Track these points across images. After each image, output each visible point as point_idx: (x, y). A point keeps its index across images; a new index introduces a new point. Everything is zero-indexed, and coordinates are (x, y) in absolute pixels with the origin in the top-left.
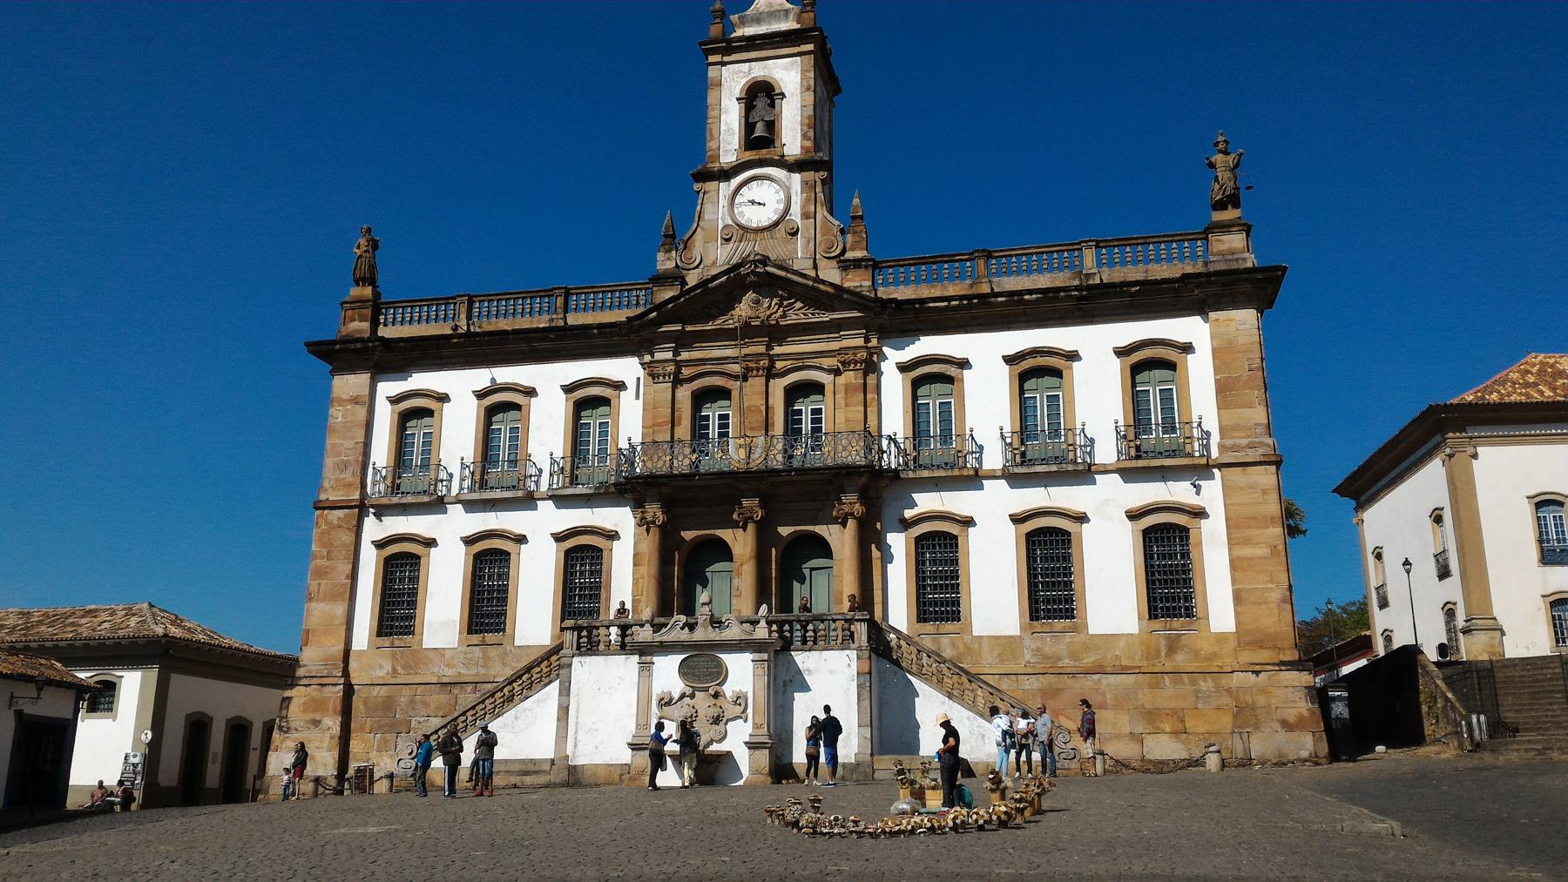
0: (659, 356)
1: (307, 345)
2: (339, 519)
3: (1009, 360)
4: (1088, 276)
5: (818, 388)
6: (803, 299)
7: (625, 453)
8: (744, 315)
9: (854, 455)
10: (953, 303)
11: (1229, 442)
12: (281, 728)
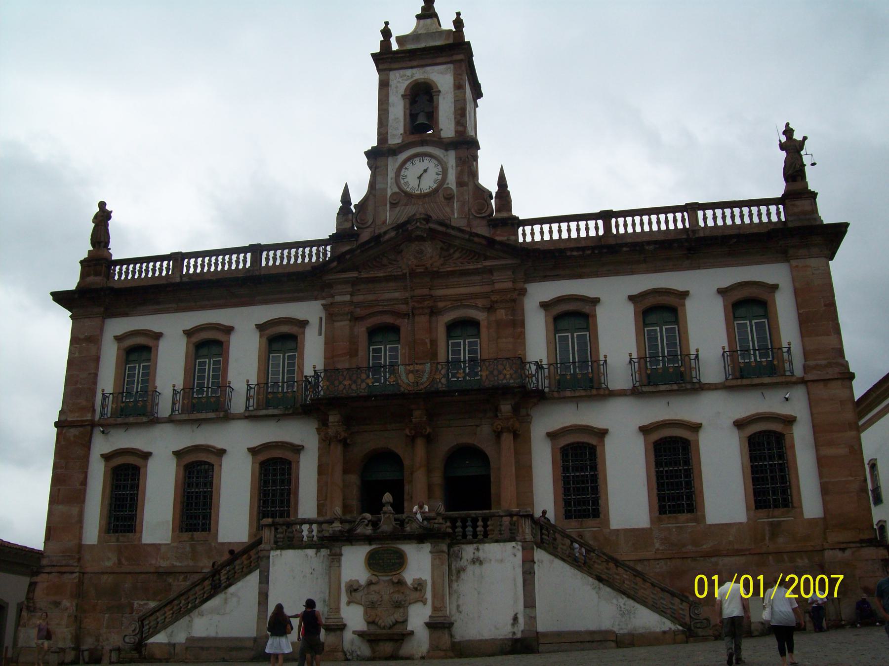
0: (338, 298)
1: (53, 294)
2: (75, 436)
3: (631, 298)
4: (694, 231)
5: (474, 324)
6: (460, 250)
7: (310, 380)
8: (410, 263)
9: (508, 377)
10: (589, 252)
11: (811, 363)
12: (28, 608)
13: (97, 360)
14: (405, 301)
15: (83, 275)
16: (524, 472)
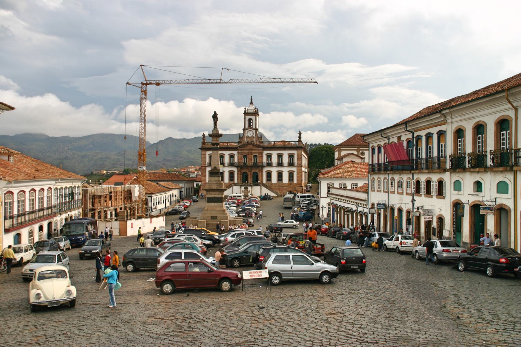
13: (206, 157)
14: (248, 152)
15: (202, 145)
16: (262, 176)
